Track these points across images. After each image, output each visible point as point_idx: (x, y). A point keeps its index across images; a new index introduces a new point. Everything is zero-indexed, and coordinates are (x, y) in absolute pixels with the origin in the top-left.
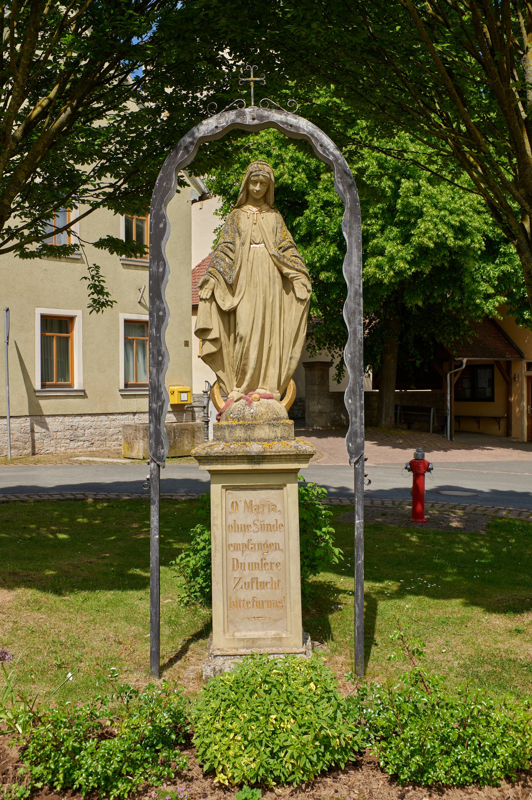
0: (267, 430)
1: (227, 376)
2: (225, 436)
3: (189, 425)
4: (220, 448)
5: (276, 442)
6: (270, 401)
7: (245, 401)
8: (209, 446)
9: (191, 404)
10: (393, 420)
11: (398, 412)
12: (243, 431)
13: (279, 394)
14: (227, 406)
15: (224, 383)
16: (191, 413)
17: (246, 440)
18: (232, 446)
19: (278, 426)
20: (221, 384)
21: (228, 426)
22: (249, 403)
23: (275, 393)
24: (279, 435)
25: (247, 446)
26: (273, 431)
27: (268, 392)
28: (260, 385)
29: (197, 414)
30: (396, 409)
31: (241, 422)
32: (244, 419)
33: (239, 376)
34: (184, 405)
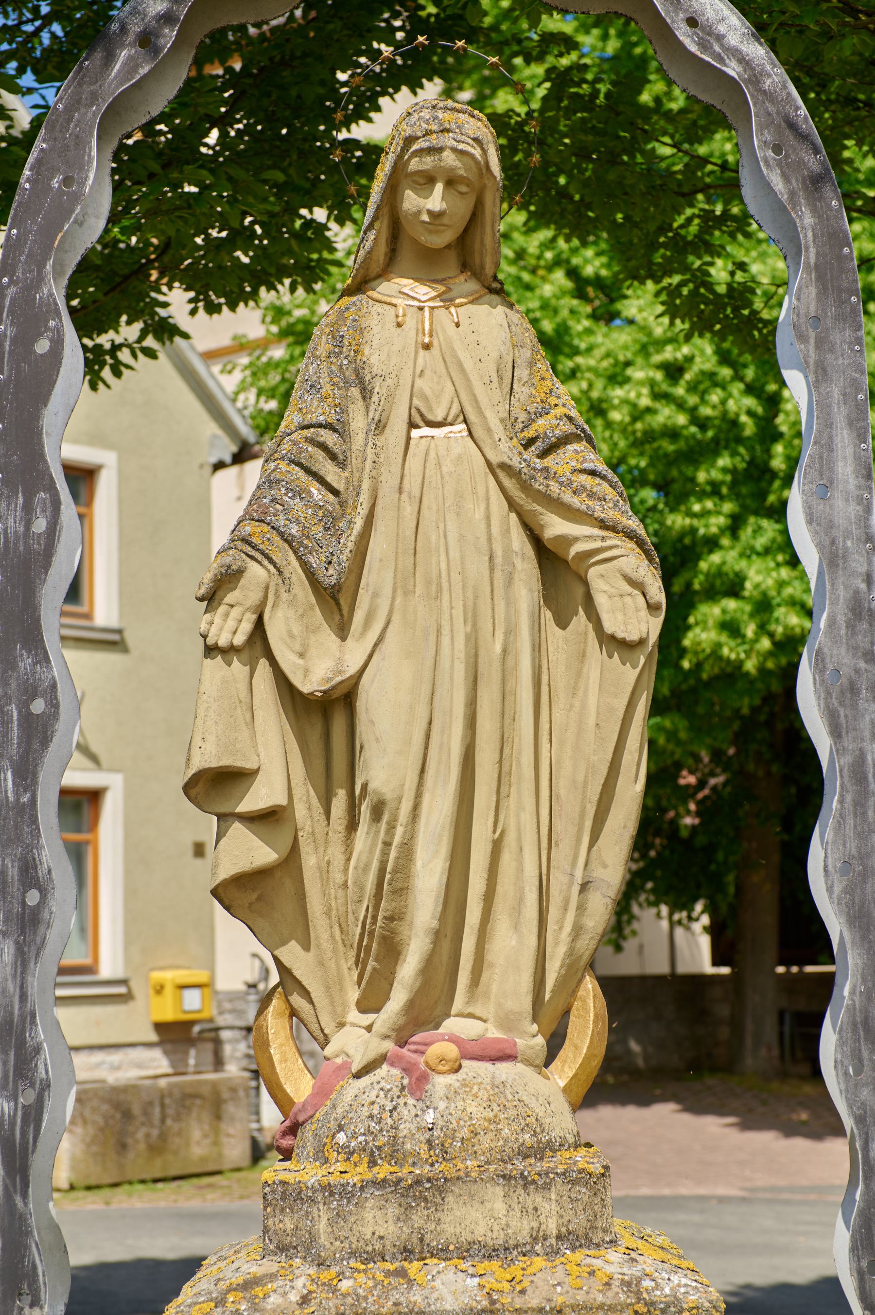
0: (500, 1206)
1: (321, 964)
2: (313, 1237)
3: (206, 1082)
4: (294, 1297)
5: (539, 1262)
6: (504, 1069)
7: (396, 1072)
8: (248, 1285)
9: (211, 1020)
10: (776, 1052)
11: (787, 1028)
12: (393, 1210)
13: (540, 1040)
14: (322, 1093)
15: (306, 994)
16: (209, 1046)
17: (407, 1253)
18: (345, 1285)
19: (547, 1187)
20: (297, 1000)
21: (328, 1189)
22: (417, 1082)
23: (523, 1034)
24: (552, 1226)
25: (410, 1282)
26: (524, 1210)
27: (494, 1033)
28: (458, 1004)
29: (227, 1049)
30: (781, 1022)
31: (383, 1171)
32: (395, 1152)
33: (371, 964)
34: (191, 1023)
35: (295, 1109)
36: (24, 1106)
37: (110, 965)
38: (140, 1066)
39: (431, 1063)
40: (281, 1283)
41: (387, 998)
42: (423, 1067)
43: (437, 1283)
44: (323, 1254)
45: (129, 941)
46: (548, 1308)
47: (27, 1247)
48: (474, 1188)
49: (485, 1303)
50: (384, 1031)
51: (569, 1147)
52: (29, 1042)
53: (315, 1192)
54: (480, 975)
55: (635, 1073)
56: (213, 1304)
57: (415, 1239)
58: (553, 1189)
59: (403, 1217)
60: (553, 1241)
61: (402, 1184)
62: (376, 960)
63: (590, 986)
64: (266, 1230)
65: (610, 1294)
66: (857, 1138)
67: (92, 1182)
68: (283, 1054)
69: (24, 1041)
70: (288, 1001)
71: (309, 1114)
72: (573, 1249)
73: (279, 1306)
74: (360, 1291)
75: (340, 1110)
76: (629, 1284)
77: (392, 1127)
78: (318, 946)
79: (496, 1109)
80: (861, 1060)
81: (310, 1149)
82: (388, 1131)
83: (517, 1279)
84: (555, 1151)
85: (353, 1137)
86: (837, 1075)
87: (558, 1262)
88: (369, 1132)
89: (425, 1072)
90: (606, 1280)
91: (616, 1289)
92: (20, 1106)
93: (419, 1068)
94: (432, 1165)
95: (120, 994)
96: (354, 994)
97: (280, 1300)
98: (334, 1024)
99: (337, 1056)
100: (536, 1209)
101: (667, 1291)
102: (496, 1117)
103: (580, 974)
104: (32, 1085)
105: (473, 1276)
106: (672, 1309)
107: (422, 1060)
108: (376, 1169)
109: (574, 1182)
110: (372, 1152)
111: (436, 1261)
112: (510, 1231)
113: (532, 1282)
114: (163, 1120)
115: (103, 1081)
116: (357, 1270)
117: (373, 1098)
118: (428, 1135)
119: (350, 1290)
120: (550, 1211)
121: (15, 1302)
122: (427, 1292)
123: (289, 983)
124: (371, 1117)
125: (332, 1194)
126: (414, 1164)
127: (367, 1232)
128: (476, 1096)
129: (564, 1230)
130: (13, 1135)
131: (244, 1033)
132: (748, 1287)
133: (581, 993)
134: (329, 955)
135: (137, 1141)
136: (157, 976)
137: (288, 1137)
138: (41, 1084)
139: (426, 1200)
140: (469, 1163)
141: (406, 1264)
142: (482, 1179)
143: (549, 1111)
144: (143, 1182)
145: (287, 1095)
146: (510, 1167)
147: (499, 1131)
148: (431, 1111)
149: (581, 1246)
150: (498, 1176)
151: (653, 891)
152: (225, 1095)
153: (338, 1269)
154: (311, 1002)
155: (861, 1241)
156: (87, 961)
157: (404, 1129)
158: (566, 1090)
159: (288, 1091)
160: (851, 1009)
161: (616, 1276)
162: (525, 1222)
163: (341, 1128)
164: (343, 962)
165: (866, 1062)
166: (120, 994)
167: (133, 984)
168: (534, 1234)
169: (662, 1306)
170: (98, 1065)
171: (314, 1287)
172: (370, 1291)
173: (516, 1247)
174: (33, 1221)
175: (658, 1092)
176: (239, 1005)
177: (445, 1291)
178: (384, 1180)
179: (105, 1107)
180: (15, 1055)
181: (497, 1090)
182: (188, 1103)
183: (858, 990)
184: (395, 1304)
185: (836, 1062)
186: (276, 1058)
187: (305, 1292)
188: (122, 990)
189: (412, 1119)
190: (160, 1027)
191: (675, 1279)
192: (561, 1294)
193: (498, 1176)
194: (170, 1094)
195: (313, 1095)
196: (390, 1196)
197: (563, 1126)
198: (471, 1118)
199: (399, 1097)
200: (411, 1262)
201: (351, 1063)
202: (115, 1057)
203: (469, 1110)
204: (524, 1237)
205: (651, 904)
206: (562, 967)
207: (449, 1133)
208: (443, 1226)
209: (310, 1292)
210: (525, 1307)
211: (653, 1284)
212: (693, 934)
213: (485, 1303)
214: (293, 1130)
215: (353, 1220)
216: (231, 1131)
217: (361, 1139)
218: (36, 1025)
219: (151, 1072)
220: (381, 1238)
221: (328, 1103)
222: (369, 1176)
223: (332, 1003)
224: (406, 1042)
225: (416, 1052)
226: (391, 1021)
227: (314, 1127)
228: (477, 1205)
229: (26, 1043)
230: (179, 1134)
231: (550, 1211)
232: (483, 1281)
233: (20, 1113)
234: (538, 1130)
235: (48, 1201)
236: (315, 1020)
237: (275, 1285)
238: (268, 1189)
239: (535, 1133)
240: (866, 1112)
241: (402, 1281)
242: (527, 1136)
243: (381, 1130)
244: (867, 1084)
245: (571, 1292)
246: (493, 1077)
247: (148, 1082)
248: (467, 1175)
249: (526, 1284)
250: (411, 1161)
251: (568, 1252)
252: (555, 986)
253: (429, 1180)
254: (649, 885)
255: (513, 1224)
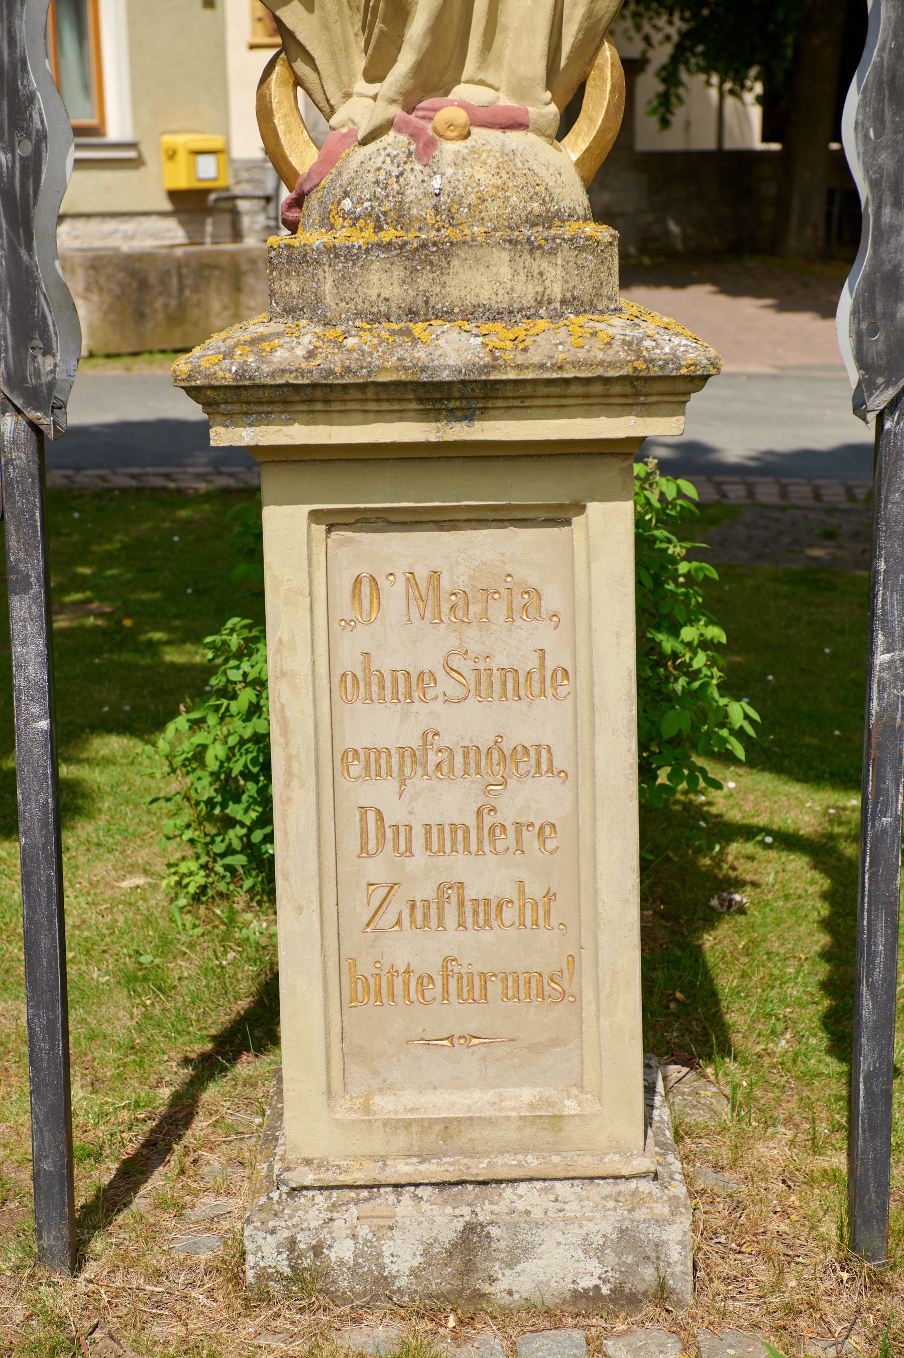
0: (505, 271)
1: (326, 27)
2: (319, 298)
3: (224, 252)
4: (300, 352)
5: (542, 324)
6: (514, 138)
7: (403, 138)
8: (253, 342)
9: (227, 189)
10: (821, 233)
11: (836, 209)
12: (398, 272)
13: (553, 109)
14: (328, 161)
15: (310, 60)
16: (227, 217)
17: (412, 314)
18: (351, 342)
19: (553, 252)
20: (301, 67)
21: (333, 251)
22: (425, 148)
23: (535, 101)
24: (556, 291)
25: (415, 341)
26: (529, 275)
27: (504, 100)
28: (469, 69)
29: (246, 221)
30: (830, 202)
31: (389, 235)
32: (401, 218)
33: (379, 26)
34: (207, 191)
35: (300, 180)
36: (21, 158)
37: (117, 128)
38: (154, 236)
39: (439, 128)
40: (287, 339)
41: (394, 61)
42: (430, 132)
43: (442, 342)
44: (329, 314)
45: (137, 101)
46: (549, 364)
47: (35, 299)
48: (480, 252)
49: (488, 359)
50: (391, 94)
51: (578, 219)
52: (22, 91)
53: (320, 254)
54: (492, 39)
55: (672, 255)
56: (221, 356)
57: (420, 301)
58: (559, 254)
59: (408, 280)
60: (558, 305)
61: (408, 248)
62: (384, 21)
63: (608, 53)
64: (272, 294)
65: (610, 352)
66: (870, 203)
67: (112, 350)
68: (288, 125)
69: (17, 90)
70: (291, 68)
71: (314, 182)
72: (577, 314)
73: (285, 359)
74: (366, 348)
75: (345, 177)
76: (630, 344)
77: (398, 193)
78: (322, 7)
79: (505, 176)
80: (882, 122)
81: (315, 216)
82: (394, 197)
83: (520, 339)
84: (563, 221)
85: (358, 202)
86: (856, 138)
87: (561, 323)
88: (375, 197)
89: (432, 137)
90: (608, 340)
91: (617, 348)
92: (17, 157)
93: (426, 134)
94: (438, 230)
95: (127, 157)
96: (360, 63)
97: (287, 354)
98: (340, 95)
99: (343, 126)
100: (541, 274)
101: (667, 350)
102: (504, 184)
103: (598, 40)
104: (29, 136)
105: (476, 336)
106: (671, 366)
107: (429, 127)
108: (381, 234)
109: (581, 249)
110: (378, 218)
111: (440, 322)
112: (515, 295)
113: (535, 341)
114: (181, 290)
115: (117, 249)
116: (362, 329)
117: (380, 164)
118: (434, 200)
119: (356, 347)
120: (555, 276)
121: (27, 351)
122: (430, 349)
123: (292, 48)
124: (377, 182)
125: (337, 256)
126: (420, 229)
127: (373, 294)
128: (484, 163)
129: (568, 295)
130: (13, 187)
131: (262, 203)
132: (770, 453)
133: (599, 61)
134: (334, 17)
135: (155, 311)
136: (168, 139)
137: (294, 210)
138: (37, 135)
139: (431, 263)
140: (475, 229)
141: (411, 325)
142: (488, 244)
143: (559, 181)
144: (163, 352)
145: (292, 167)
146: (516, 233)
147: (507, 198)
148: (438, 177)
149: (585, 311)
150: (504, 241)
151: (704, 54)
152: (245, 267)
153: (343, 328)
154: (316, 69)
155: (864, 304)
156: (93, 121)
157: (411, 194)
158: (579, 164)
159: (294, 163)
160: (879, 67)
161: (617, 337)
162: (530, 286)
163: (346, 194)
164: (349, 27)
165: (888, 125)
166: (127, 157)
167: (143, 147)
168: (539, 298)
169: (661, 363)
170: (112, 233)
171: (320, 344)
172: (376, 347)
173: (520, 310)
174: (40, 273)
175: (695, 274)
176: (257, 174)
177: (448, 349)
178: (390, 243)
179: (120, 275)
180: (8, 104)
181: (506, 158)
182: (206, 273)
183: (888, 45)
184: (399, 359)
185: (856, 123)
186: (281, 129)
187: (311, 347)
188: (131, 154)
189: (419, 184)
190: (174, 195)
191: (676, 340)
192: (562, 352)
193: (504, 241)
194: (187, 264)
195: (318, 163)
196: (396, 259)
197: (573, 197)
198: (479, 185)
199: (405, 163)
200: (417, 322)
201: (357, 131)
202: (129, 226)
203: (477, 177)
204: (528, 301)
205: (700, 69)
206: (579, 30)
207: (457, 199)
208: (448, 289)
209: (316, 348)
210: (526, 363)
211: (654, 344)
212: (743, 103)
213: (488, 359)
214: (298, 202)
215: (358, 281)
216: (252, 304)
217: (367, 204)
218: (28, 73)
219: (167, 242)
220: (387, 300)
221: (334, 171)
222: (375, 239)
223: (338, 71)
224: (414, 109)
225: (424, 118)
226: (399, 84)
227: (319, 195)
228: (482, 269)
229: (18, 91)
230: (198, 305)
231: (555, 276)
232: (487, 340)
233: (18, 165)
234: (547, 199)
235: (54, 260)
236: (320, 90)
237: (282, 341)
238: (273, 253)
239: (544, 203)
240: (882, 177)
241: (406, 339)
242: (535, 205)
243: (387, 196)
244: (886, 148)
245: (573, 350)
246: (503, 145)
247: (164, 251)
248: (473, 240)
249: (528, 342)
250: (417, 226)
251: (572, 316)
252: (571, 52)
253: (435, 244)
254: (700, 48)
255: (518, 288)
